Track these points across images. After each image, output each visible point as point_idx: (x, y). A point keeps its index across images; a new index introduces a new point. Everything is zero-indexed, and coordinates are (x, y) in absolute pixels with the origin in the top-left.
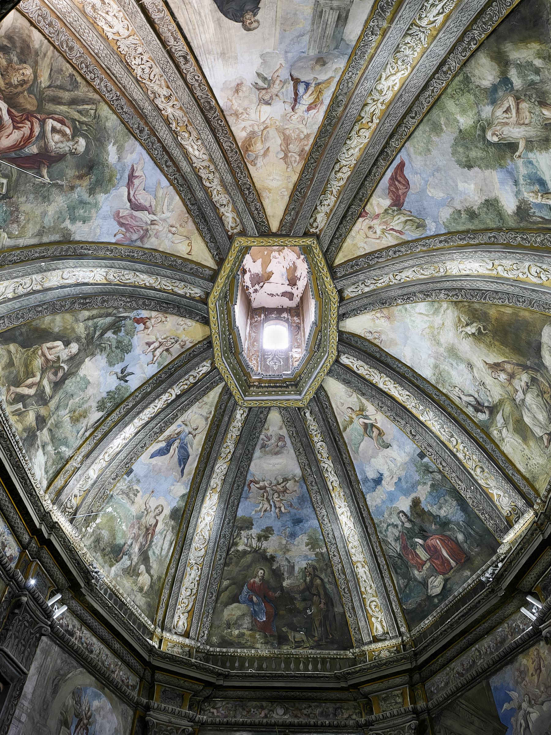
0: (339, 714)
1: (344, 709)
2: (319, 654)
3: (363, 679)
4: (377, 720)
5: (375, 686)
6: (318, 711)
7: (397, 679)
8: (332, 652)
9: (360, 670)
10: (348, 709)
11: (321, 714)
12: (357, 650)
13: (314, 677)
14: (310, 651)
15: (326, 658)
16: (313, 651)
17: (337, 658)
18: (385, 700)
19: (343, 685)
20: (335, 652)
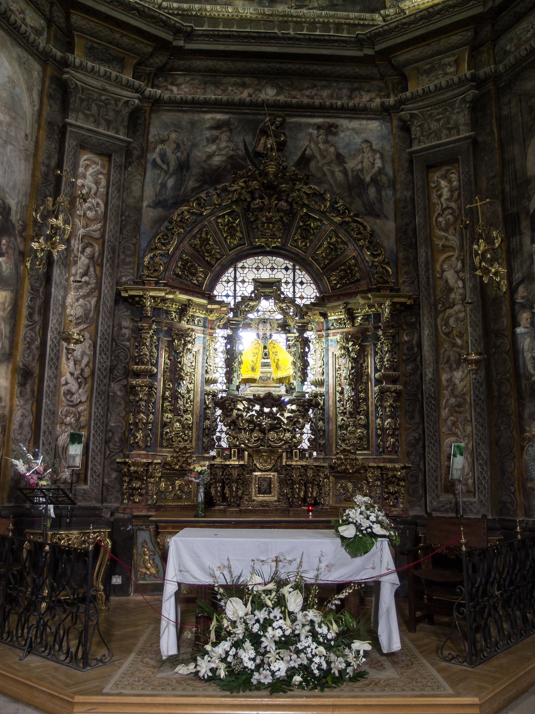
0: (356, 97)
1: (364, 91)
2: (333, 17)
3: (399, 40)
4: (414, 99)
5: (416, 52)
6: (325, 93)
7: (455, 37)
8: (352, 15)
9: (396, 27)
10: (369, 91)
11: (331, 96)
12: (391, 10)
13: (325, 40)
14: (318, 12)
15: (341, 24)
16: (324, 13)
17: (359, 25)
18: (427, 72)
19: (369, 52)
20: (357, 14)
